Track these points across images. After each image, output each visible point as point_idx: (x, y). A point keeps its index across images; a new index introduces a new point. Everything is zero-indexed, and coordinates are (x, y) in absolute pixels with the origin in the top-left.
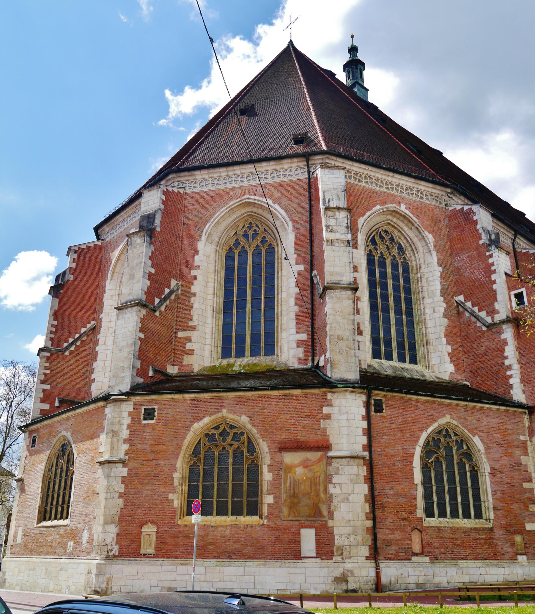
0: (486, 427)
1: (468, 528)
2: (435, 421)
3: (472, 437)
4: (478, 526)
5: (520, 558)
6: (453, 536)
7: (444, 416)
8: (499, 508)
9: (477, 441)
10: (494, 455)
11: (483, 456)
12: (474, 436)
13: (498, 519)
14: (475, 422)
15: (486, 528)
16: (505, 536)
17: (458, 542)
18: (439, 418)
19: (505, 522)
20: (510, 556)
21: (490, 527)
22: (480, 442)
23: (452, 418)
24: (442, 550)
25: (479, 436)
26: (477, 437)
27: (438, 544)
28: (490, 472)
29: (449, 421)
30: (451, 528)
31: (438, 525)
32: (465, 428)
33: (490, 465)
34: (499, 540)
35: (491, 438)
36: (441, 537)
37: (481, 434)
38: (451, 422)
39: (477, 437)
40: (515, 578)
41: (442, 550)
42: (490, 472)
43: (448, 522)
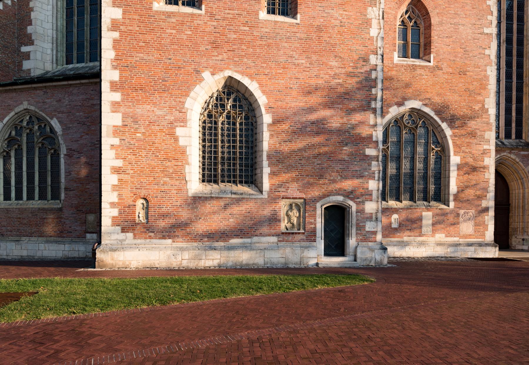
0: (68, 107)
1: (36, 208)
2: (12, 110)
3: (49, 120)
4: (46, 207)
5: (88, 236)
6: (20, 216)
7: (22, 103)
8: (72, 189)
9: (55, 124)
10: (73, 135)
11: (60, 138)
12: (52, 119)
13: (69, 199)
14: (55, 103)
15: (55, 208)
16: (74, 215)
17: (25, 222)
18: (16, 107)
19: (76, 202)
20: (78, 234)
21: (58, 207)
22: (58, 124)
23: (29, 104)
24: (8, 228)
25: (57, 118)
26: (55, 119)
27: (5, 223)
28: (65, 153)
29: (25, 107)
30: (19, 209)
31: (6, 207)
32: (43, 112)
33: (66, 146)
34: (68, 219)
35: (72, 117)
36: (9, 217)
37: (60, 115)
38: (28, 108)
39: (55, 119)
40: (76, 255)
41: (8, 228)
42: (65, 153)
43: (25, 203)
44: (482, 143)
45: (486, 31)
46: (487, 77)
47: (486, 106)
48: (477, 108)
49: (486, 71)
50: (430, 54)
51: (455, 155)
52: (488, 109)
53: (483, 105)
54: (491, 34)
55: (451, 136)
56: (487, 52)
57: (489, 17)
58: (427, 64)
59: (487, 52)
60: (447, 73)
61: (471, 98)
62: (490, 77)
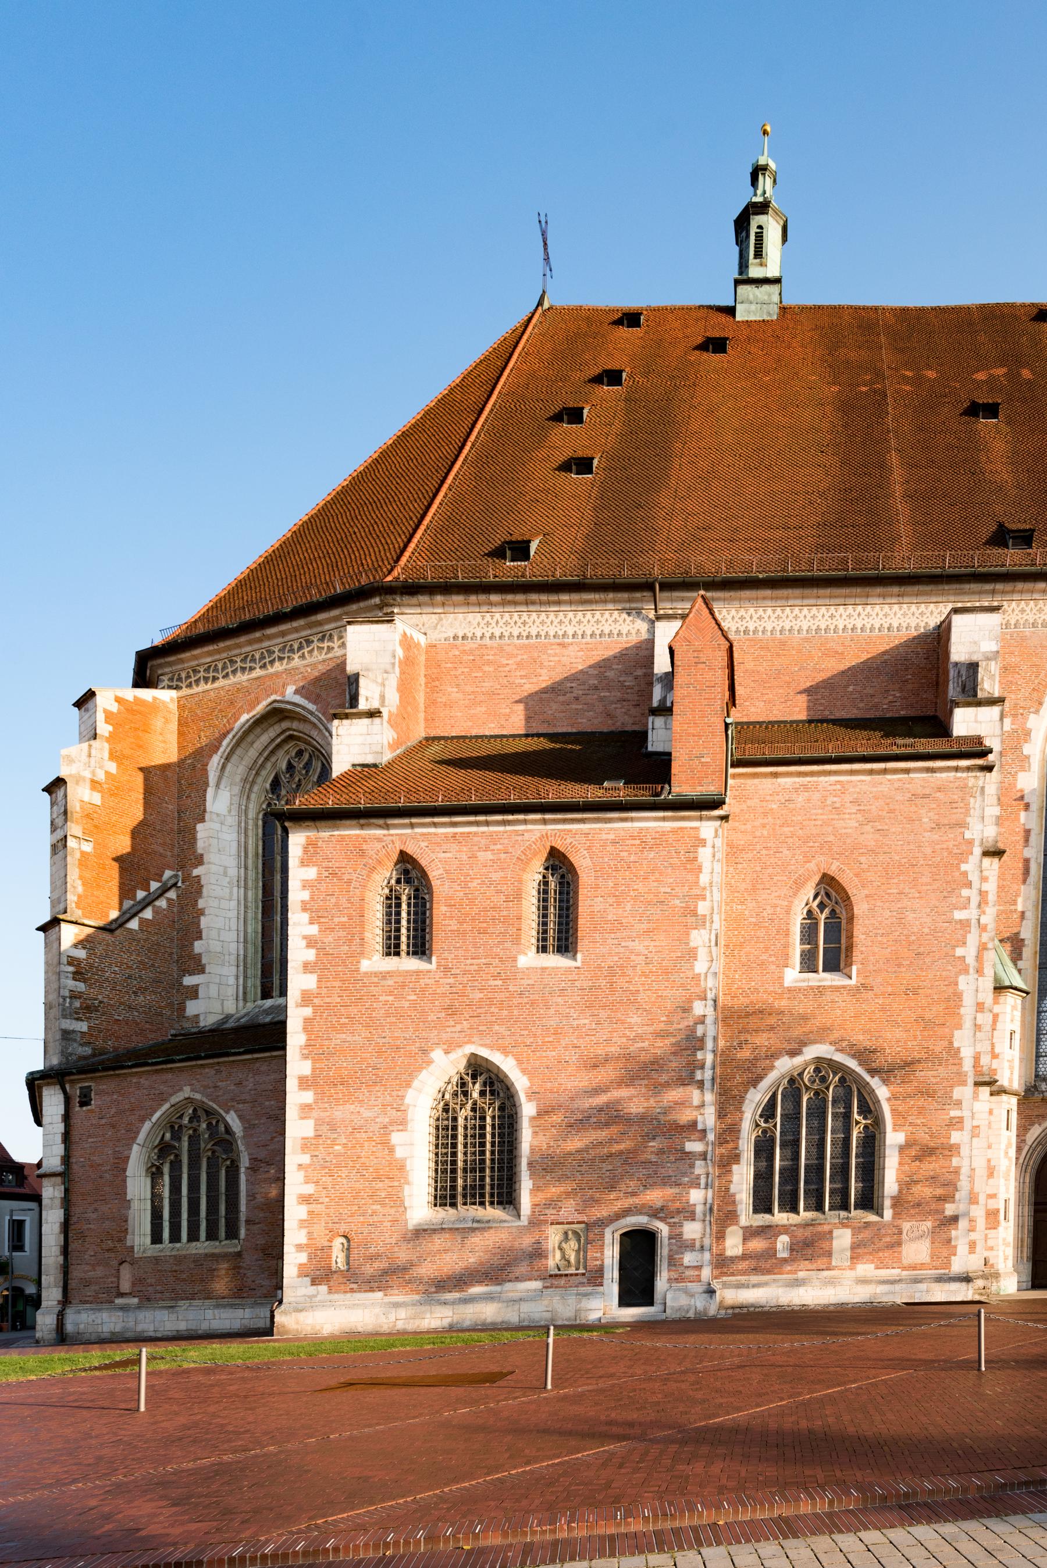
44: (948, 1107)
45: (958, 915)
46: (958, 996)
47: (956, 1045)
48: (938, 1049)
49: (956, 984)
50: (851, 965)
51: (894, 1130)
52: (959, 1049)
53: (951, 1043)
54: (968, 921)
55: (889, 1100)
56: (959, 952)
57: (965, 892)
58: (846, 982)
59: (959, 952)
60: (883, 994)
61: (926, 1033)
62: (965, 995)
